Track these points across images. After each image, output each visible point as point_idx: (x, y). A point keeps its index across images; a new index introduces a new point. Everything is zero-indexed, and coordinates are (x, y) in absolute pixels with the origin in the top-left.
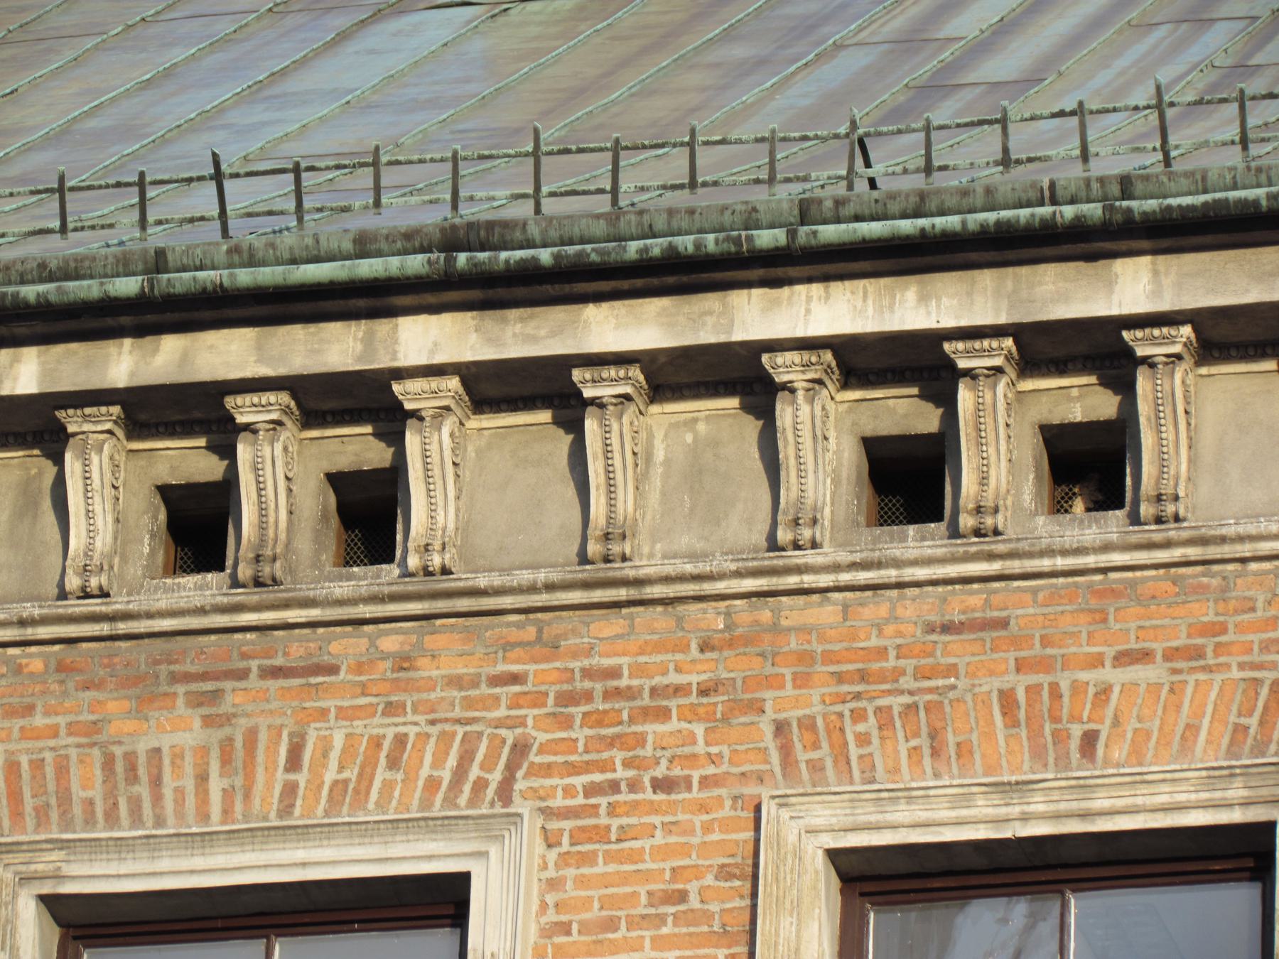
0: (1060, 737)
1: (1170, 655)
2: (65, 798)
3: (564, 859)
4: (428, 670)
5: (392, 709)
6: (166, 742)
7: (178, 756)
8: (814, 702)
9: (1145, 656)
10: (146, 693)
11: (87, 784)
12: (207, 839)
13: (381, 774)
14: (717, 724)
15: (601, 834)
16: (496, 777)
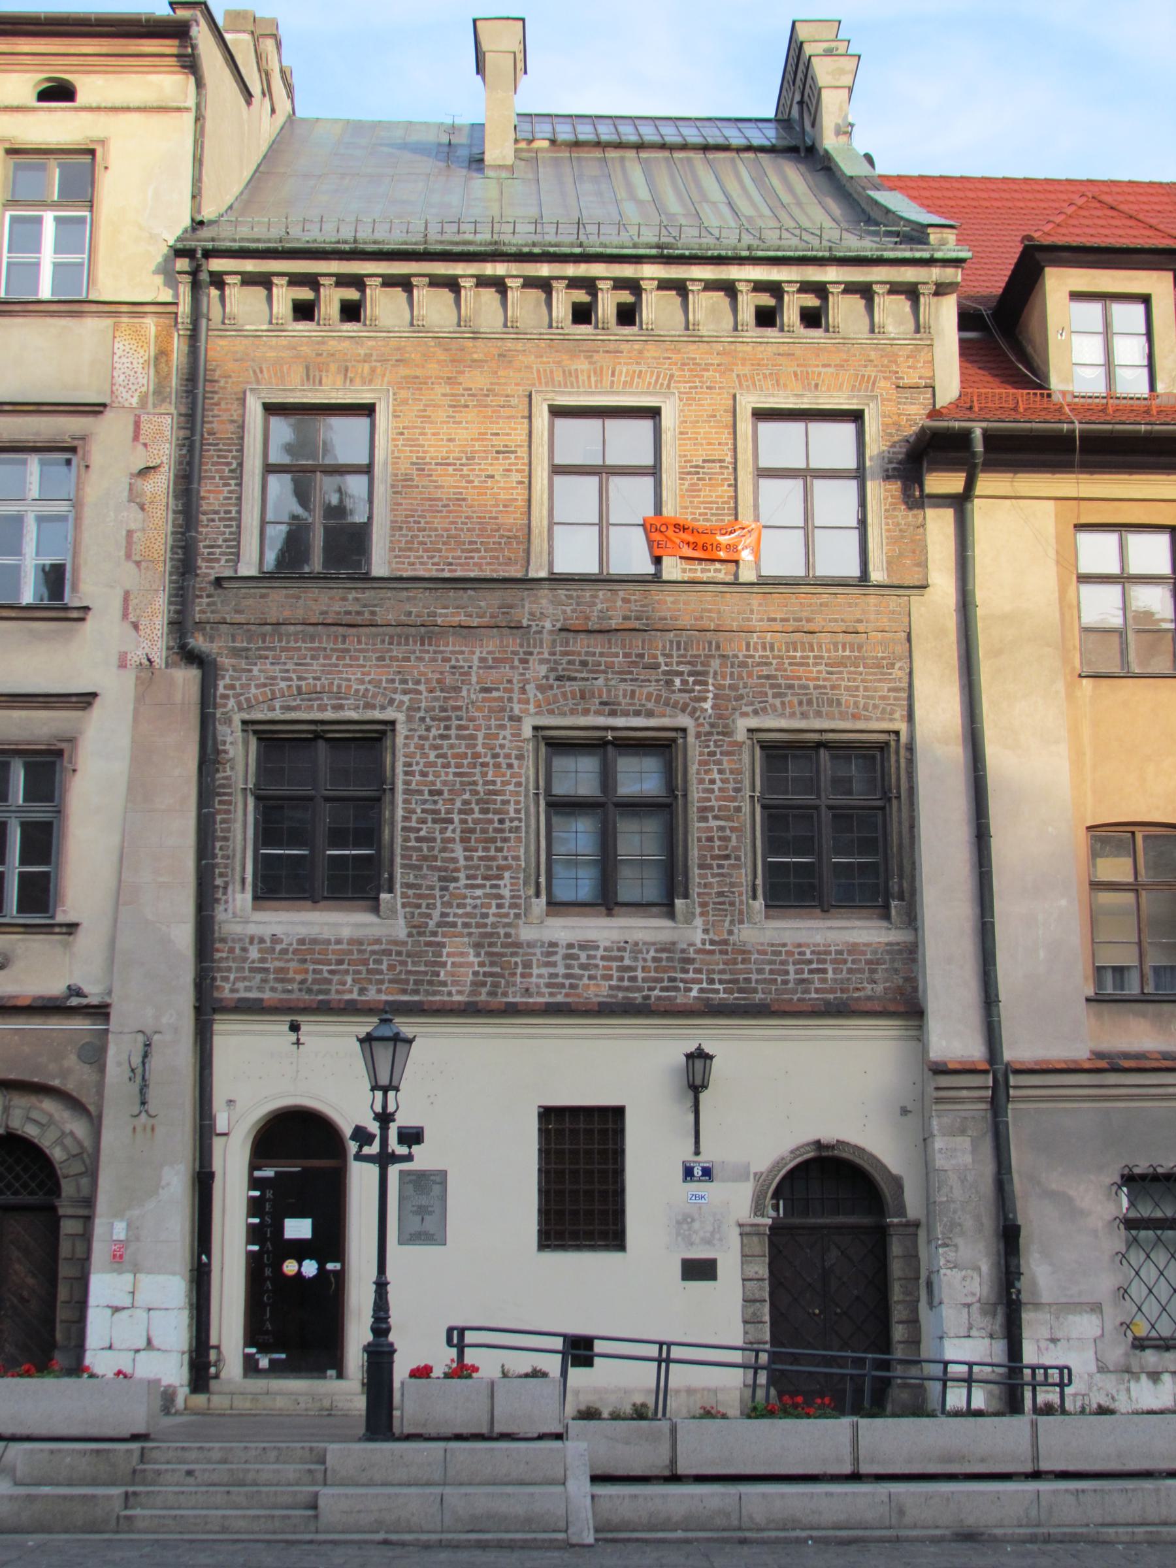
0: (809, 384)
1: (836, 366)
2: (553, 379)
3: (684, 405)
4: (647, 355)
5: (638, 363)
6: (579, 367)
7: (582, 371)
8: (746, 370)
9: (829, 366)
10: (573, 355)
11: (559, 377)
12: (592, 393)
13: (636, 380)
14: (722, 374)
15: (694, 399)
16: (666, 382)
